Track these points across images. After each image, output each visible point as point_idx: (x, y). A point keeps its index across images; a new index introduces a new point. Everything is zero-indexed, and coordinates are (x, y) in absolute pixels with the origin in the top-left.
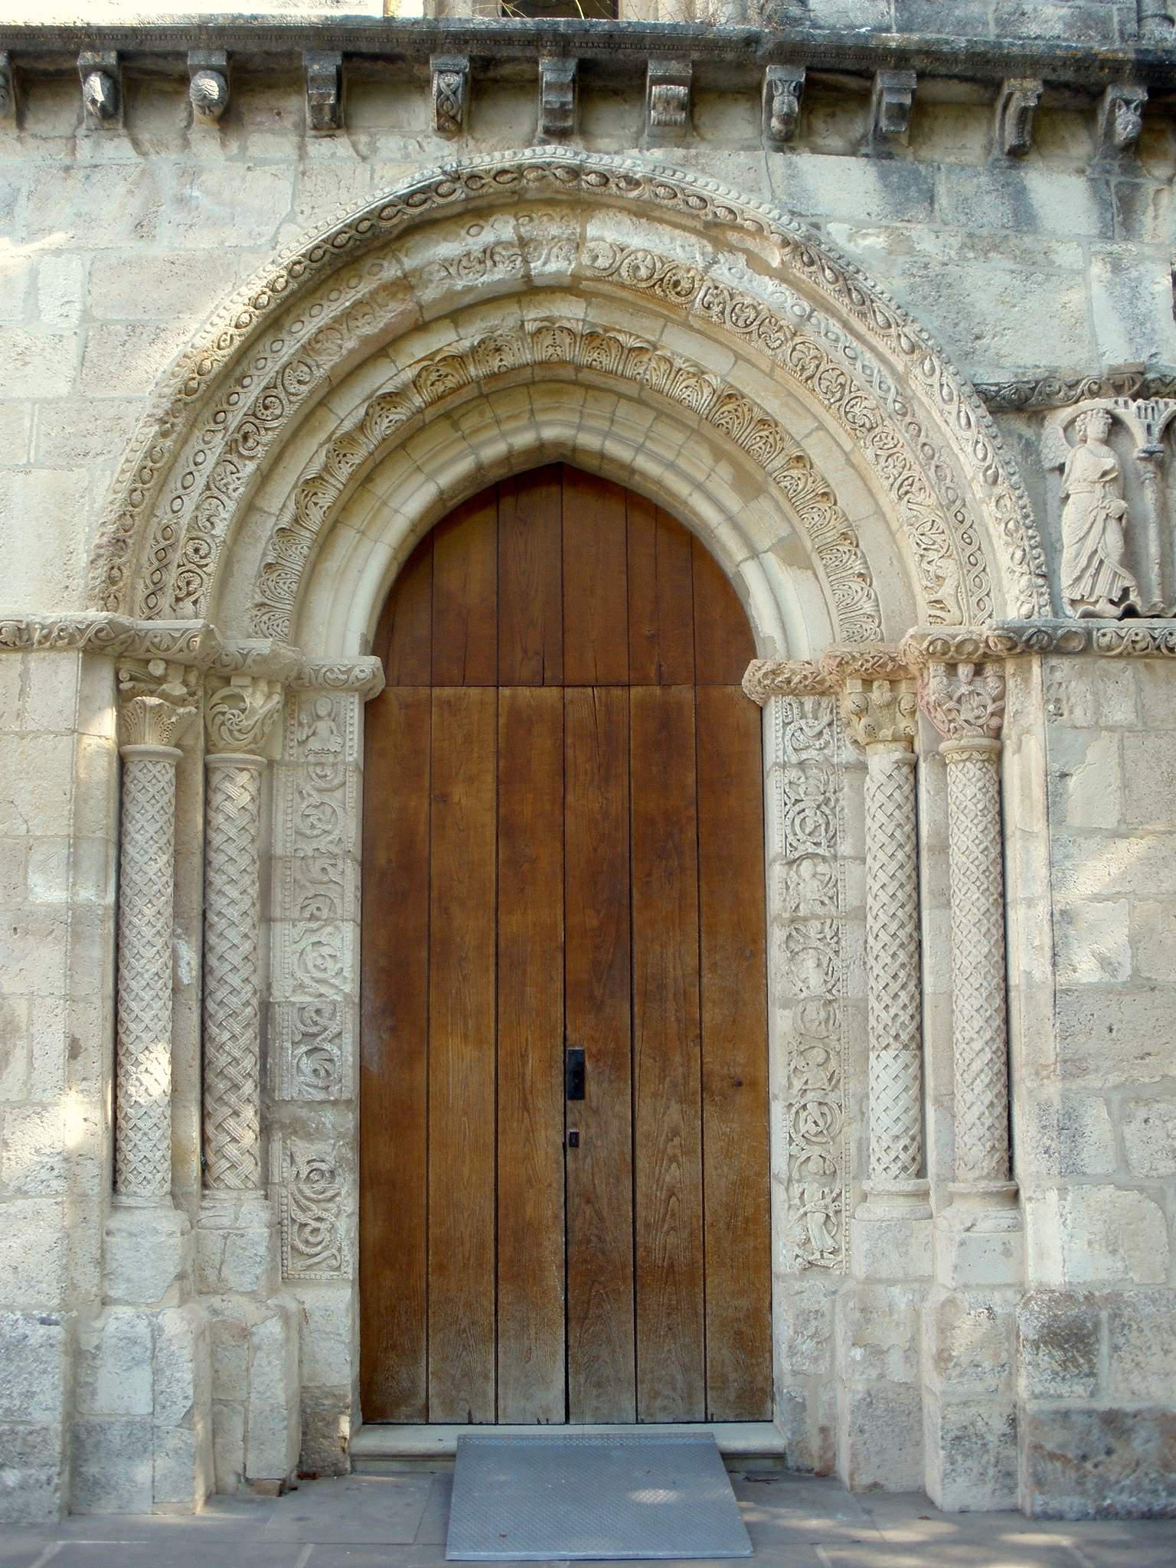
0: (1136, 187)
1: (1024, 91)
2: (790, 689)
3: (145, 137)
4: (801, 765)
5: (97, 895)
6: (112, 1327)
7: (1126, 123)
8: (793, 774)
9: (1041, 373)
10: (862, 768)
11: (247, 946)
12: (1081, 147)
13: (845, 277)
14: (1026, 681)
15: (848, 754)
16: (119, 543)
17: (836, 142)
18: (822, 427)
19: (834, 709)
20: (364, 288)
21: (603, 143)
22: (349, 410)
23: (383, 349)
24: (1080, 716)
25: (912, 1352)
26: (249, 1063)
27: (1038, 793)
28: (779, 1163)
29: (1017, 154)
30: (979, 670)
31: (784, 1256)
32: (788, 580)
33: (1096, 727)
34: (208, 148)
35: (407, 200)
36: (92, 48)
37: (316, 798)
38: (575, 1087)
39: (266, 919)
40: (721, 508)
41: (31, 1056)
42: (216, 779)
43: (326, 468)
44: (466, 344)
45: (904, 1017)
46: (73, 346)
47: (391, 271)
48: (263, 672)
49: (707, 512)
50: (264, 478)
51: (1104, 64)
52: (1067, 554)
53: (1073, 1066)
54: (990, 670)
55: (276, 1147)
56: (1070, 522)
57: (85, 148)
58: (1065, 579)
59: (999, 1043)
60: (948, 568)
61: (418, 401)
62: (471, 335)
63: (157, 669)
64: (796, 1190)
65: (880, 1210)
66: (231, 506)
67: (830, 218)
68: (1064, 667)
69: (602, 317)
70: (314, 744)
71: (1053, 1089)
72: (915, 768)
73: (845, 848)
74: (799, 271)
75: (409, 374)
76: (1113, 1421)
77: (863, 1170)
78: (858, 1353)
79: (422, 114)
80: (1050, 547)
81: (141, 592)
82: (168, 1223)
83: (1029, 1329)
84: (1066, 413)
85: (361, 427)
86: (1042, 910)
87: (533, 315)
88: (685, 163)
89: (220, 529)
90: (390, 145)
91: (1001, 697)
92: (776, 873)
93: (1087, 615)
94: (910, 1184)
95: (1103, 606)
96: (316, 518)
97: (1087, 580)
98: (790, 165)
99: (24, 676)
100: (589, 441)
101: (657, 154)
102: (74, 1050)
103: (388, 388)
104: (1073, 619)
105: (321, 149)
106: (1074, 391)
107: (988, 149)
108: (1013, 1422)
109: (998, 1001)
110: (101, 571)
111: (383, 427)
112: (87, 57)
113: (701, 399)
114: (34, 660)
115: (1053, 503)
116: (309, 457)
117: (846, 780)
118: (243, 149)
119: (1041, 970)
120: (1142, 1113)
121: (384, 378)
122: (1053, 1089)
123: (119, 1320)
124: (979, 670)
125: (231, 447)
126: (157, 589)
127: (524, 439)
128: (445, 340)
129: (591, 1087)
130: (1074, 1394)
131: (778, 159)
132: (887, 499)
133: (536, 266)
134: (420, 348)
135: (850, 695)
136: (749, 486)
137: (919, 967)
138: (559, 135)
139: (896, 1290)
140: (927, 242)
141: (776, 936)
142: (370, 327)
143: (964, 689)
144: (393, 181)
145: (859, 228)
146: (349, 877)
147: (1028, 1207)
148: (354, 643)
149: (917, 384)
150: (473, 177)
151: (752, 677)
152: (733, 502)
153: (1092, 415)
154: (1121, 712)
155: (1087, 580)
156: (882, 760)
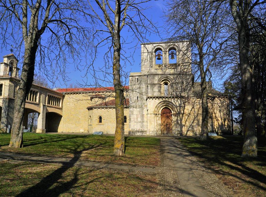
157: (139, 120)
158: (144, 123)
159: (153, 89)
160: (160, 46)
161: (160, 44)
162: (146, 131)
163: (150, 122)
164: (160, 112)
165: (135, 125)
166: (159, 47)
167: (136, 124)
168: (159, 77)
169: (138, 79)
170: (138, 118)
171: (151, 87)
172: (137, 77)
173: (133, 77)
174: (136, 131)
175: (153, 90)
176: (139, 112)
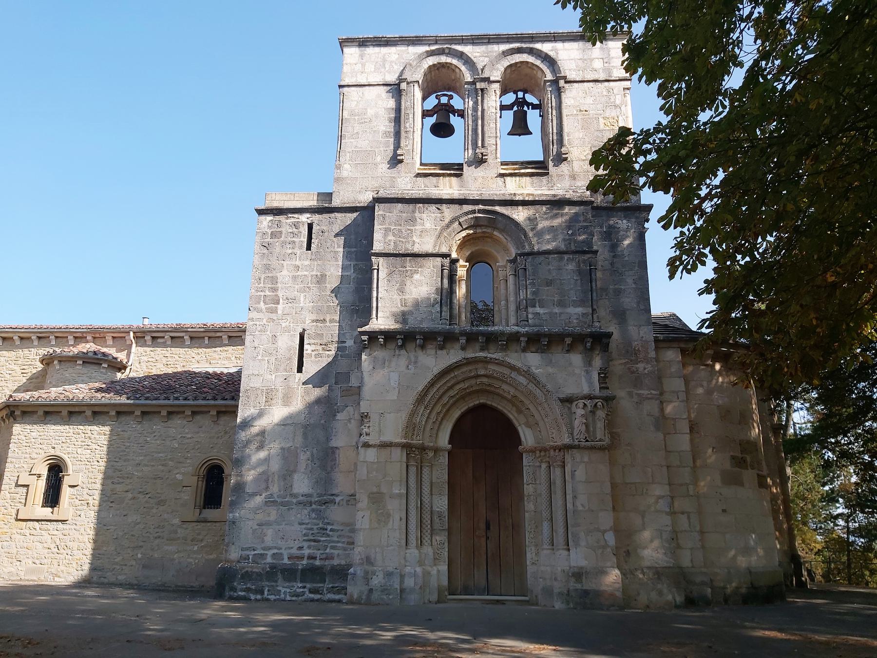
1: (568, 340)
2: (527, 451)
3: (408, 349)
5: (404, 491)
6: (407, 570)
9: (571, 395)
11: (429, 500)
14: (568, 454)
15: (538, 464)
17: (534, 349)
21: (490, 351)
22: (445, 399)
23: (451, 388)
24: (578, 460)
26: (429, 522)
27: (570, 474)
30: (560, 451)
34: (420, 353)
35: (456, 363)
37: (440, 471)
38: (488, 527)
39: (432, 494)
40: (514, 416)
41: (393, 520)
42: (423, 468)
43: (441, 410)
45: (549, 515)
46: (397, 390)
47: (453, 375)
48: (431, 449)
49: (511, 417)
50: (430, 412)
51: (583, 335)
55: (433, 538)
56: (576, 423)
58: (575, 434)
59: (565, 520)
64: (530, 548)
67: (531, 366)
68: (575, 451)
69: (490, 381)
70: (440, 461)
73: (537, 482)
78: (541, 580)
79: (457, 346)
80: (572, 428)
81: (410, 435)
82: (417, 551)
84: (576, 402)
85: (448, 402)
86: (571, 496)
87: (479, 381)
88: (506, 355)
90: (452, 351)
92: (525, 486)
94: (550, 547)
95: (582, 440)
96: (439, 419)
99: (391, 451)
100: (489, 403)
102: (401, 519)
104: (576, 443)
105: (439, 352)
106: (578, 399)
108: (568, 591)
109: (565, 512)
112: (398, 337)
113: (509, 397)
114: (392, 448)
115: (574, 419)
116: (438, 408)
119: (571, 507)
121: (452, 393)
123: (408, 569)
124: (560, 451)
127: (477, 402)
128: (462, 385)
129: (491, 527)
130: (579, 586)
131: (522, 354)
133: (479, 373)
134: (458, 387)
135: (538, 452)
136: (520, 411)
138: (482, 349)
140: (550, 370)
141: (526, 498)
142: (449, 385)
143: (557, 454)
148: (447, 442)
151: (520, 448)
152: (516, 415)
153: (581, 403)
154: (586, 459)
156: (544, 466)
157: (302, 485)
158: (333, 507)
159: (403, 284)
162: (341, 573)
163: (377, 499)
164: (444, 440)
165: (268, 524)
166: (444, 59)
167: (273, 513)
169: (310, 227)
170: (295, 471)
171: (390, 274)
172: (305, 218)
173: (282, 218)
174: (273, 567)
175: (401, 290)
176: (305, 436)
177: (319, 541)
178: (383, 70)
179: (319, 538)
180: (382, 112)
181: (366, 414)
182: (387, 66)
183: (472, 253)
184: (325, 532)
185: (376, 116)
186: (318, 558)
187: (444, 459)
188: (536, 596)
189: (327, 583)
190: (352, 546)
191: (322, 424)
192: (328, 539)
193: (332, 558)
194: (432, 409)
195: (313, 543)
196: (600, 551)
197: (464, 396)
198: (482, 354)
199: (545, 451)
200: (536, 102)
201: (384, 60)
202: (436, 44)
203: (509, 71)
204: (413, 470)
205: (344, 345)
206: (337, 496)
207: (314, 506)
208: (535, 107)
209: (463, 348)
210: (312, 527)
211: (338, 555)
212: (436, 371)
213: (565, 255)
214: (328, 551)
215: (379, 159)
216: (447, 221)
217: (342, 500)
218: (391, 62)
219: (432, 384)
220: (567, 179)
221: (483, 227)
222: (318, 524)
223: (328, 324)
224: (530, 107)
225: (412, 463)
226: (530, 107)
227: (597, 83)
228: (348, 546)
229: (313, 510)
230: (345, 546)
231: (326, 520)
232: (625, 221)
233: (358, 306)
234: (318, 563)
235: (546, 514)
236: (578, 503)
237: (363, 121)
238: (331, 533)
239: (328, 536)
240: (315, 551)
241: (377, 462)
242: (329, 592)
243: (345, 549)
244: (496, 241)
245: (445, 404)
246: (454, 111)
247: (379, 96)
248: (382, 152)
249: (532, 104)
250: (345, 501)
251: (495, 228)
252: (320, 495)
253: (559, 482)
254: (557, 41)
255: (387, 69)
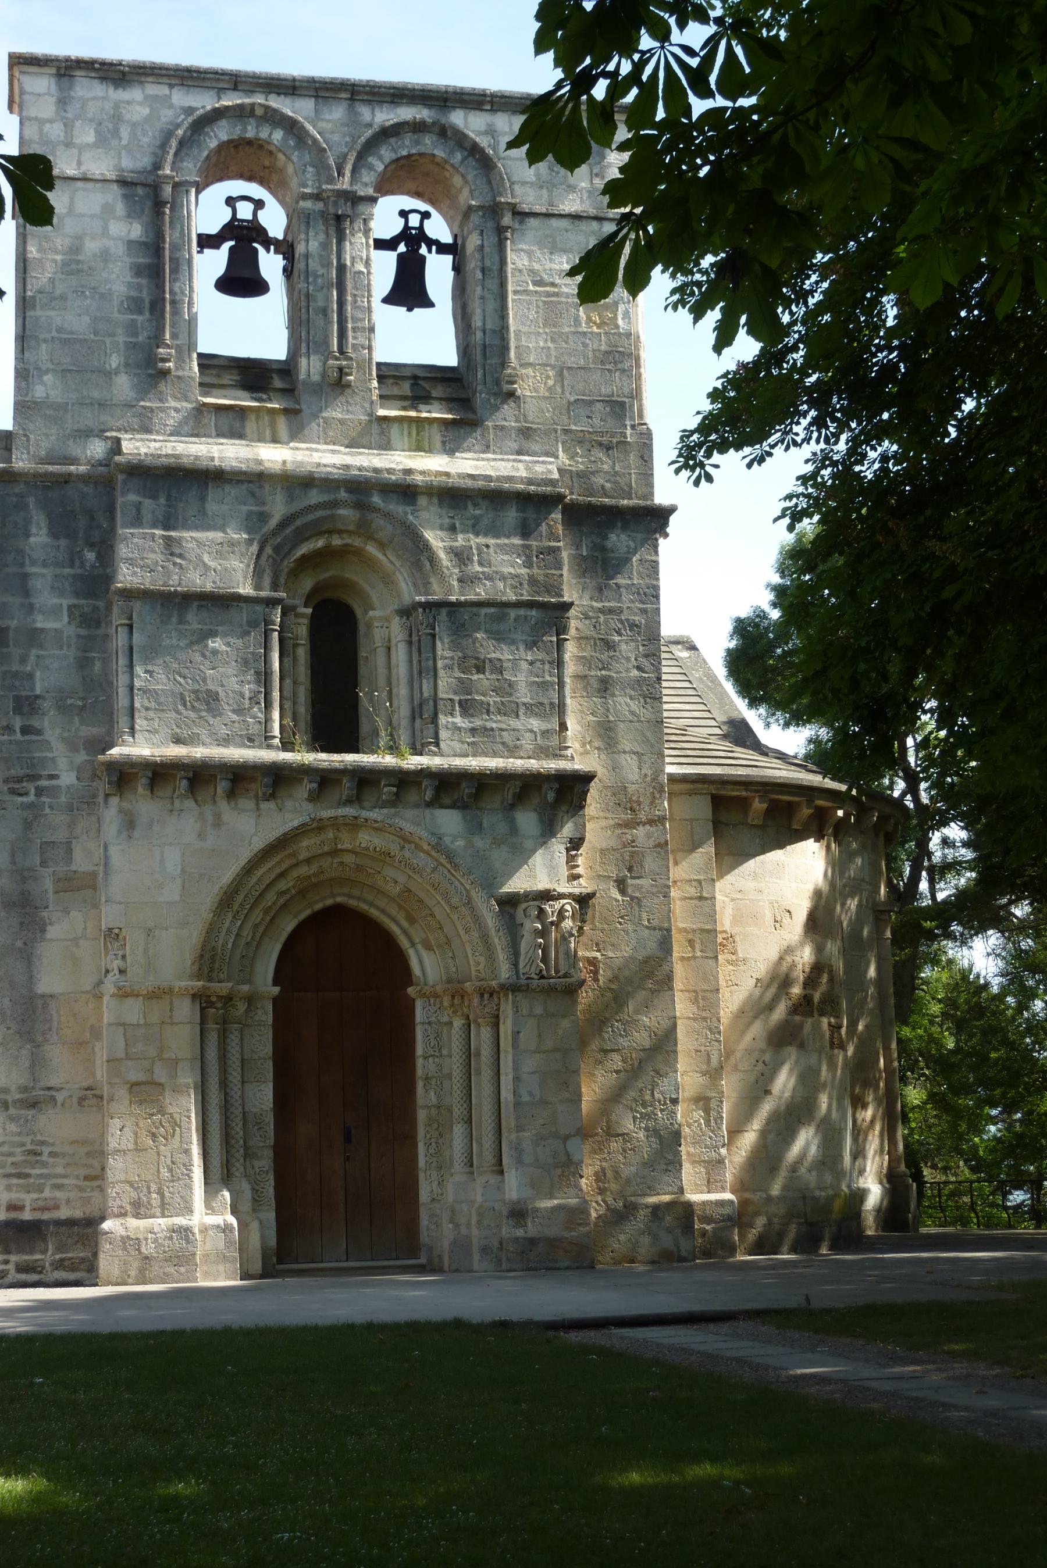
0: (555, 815)
3: (199, 799)
4: (430, 1023)
7: (551, 796)
8: (426, 1026)
10: (451, 1023)
12: (536, 801)
13: (450, 857)
14: (507, 999)
15: (446, 1019)
16: (202, 956)
17: (447, 801)
18: (439, 903)
19: (441, 1002)
20: (278, 858)
21: (366, 804)
22: (270, 897)
23: (282, 875)
25: (468, 1225)
27: (510, 1038)
28: (421, 1164)
29: (512, 806)
30: (491, 995)
31: (424, 1196)
32: (425, 955)
33: (531, 1015)
34: (223, 805)
35: (297, 828)
36: (184, 770)
37: (258, 1038)
38: (348, 1139)
44: (312, 872)
46: (179, 882)
52: (522, 957)
53: (520, 1128)
54: (495, 996)
55: (248, 1163)
57: (177, 802)
58: (521, 966)
60: (482, 959)
61: (293, 892)
62: (314, 868)
63: (214, 999)
64: (428, 1173)
65: (458, 1178)
66: (233, 937)
68: (520, 996)
70: (257, 1018)
71: (513, 1136)
72: (469, 1026)
73: (445, 1052)
74: (433, 853)
75: (291, 884)
76: (532, 1242)
77: (451, 1165)
78: (451, 1226)
80: (516, 954)
83: (505, 1213)
86: (511, 1076)
89: (230, 946)
90: (289, 804)
91: (498, 1005)
92: (420, 1062)
93: (528, 978)
94: (468, 1170)
95: (533, 976)
96: (258, 935)
97: (528, 966)
98: (432, 814)
99: (171, 1003)
101: (385, 811)
103: (284, 889)
104: (523, 981)
105: (264, 805)
107: (502, 802)
108: (501, 1244)
110: (196, 966)
111: (282, 901)
116: (257, 915)
117: (445, 1028)
118: (236, 804)
120: (543, 1143)
121: (282, 885)
122: (513, 1136)
124: (491, 995)
125: (234, 917)
126: (212, 970)
127: (329, 902)
130: (520, 1233)
131: (427, 811)
132: (462, 932)
134: (295, 873)
137: (470, 1095)
138: (349, 802)
139: (463, 1205)
140: (479, 843)
141: (420, 1085)
142: (278, 871)
144: (292, 820)
145: (455, 838)
146: (270, 1065)
147: (506, 1174)
149: (473, 894)
150: (321, 820)
151: (411, 991)
152: (405, 924)
154: (538, 1010)
155: (528, 966)
156: (458, 1023)
160: (273, 118)
161: (275, 102)
168: (263, 517)
177: (27, 1176)
178: (114, 143)
179: (27, 1171)
180: (119, 249)
181: (117, 931)
182: (125, 133)
183: (317, 583)
184: (39, 1158)
185: (105, 256)
186: (28, 1208)
187: (266, 1015)
188: (439, 1256)
189: (50, 1252)
190: (95, 1183)
191: (20, 950)
192: (45, 1171)
193: (57, 1207)
194: (246, 916)
195: (15, 1181)
196: (559, 1171)
197: (304, 891)
198: (349, 811)
199: (462, 997)
200: (447, 238)
201: (117, 118)
202: (235, 88)
203: (393, 167)
204: (213, 1037)
205: (54, 782)
206: (58, 1090)
207: (12, 1111)
208: (443, 249)
209: (314, 797)
210: (12, 1150)
211: (68, 1202)
212: (258, 844)
213: (509, 610)
214: (47, 1193)
215: (114, 361)
216: (273, 523)
217: (71, 1096)
218: (134, 125)
219: (249, 869)
220: (513, 436)
221: (344, 536)
222: (23, 1145)
223: (18, 736)
224: (434, 248)
225: (211, 1026)
226: (434, 248)
227: (577, 222)
228: (86, 1183)
229: (12, 1119)
230: (81, 1183)
231: (39, 1137)
232: (623, 537)
233: (83, 699)
234: (27, 1215)
235: (458, 1111)
236: (523, 1091)
237: (74, 267)
238: (51, 1160)
239: (44, 1165)
240: (22, 1196)
241: (145, 1024)
242: (56, 1269)
243: (81, 1189)
244: (369, 562)
245: (270, 907)
246: (267, 242)
247: (107, 210)
248: (122, 346)
249: (437, 242)
250: (75, 1101)
251: (370, 538)
252: (24, 1089)
253: (486, 1052)
254: (497, 111)
255: (124, 142)
